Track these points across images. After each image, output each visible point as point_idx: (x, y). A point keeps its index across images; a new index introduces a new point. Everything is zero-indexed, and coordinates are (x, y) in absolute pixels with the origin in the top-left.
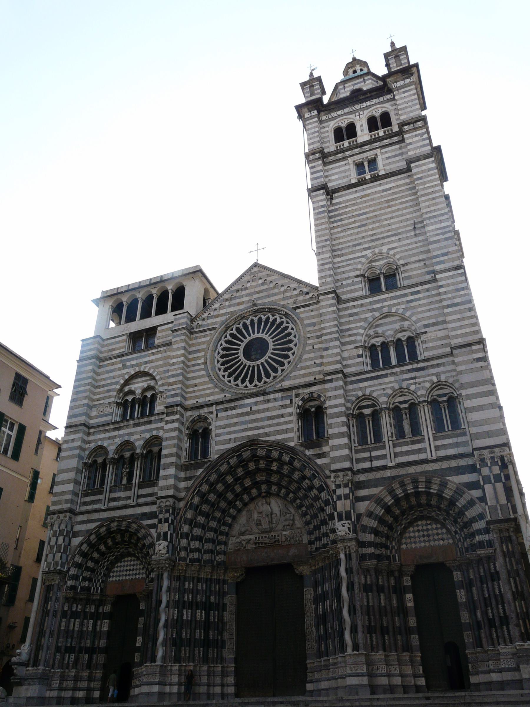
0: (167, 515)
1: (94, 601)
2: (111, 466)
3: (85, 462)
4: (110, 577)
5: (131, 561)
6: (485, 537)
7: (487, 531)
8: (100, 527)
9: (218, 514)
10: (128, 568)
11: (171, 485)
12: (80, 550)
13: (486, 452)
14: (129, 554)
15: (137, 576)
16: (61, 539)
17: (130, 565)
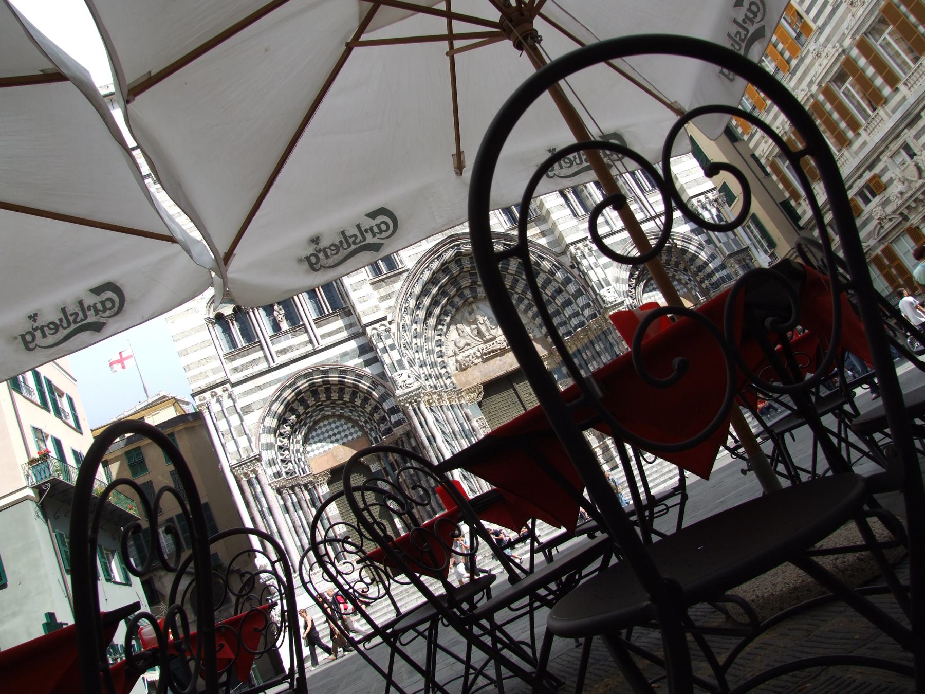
0: (389, 342)
1: (306, 486)
2: (256, 311)
3: (209, 318)
4: (309, 452)
5: (330, 424)
6: (724, 272)
7: (723, 267)
8: (283, 390)
9: (430, 333)
10: (331, 433)
11: (376, 307)
12: (264, 427)
13: (702, 198)
14: (325, 418)
15: (350, 438)
16: (235, 420)
17: (332, 429)
